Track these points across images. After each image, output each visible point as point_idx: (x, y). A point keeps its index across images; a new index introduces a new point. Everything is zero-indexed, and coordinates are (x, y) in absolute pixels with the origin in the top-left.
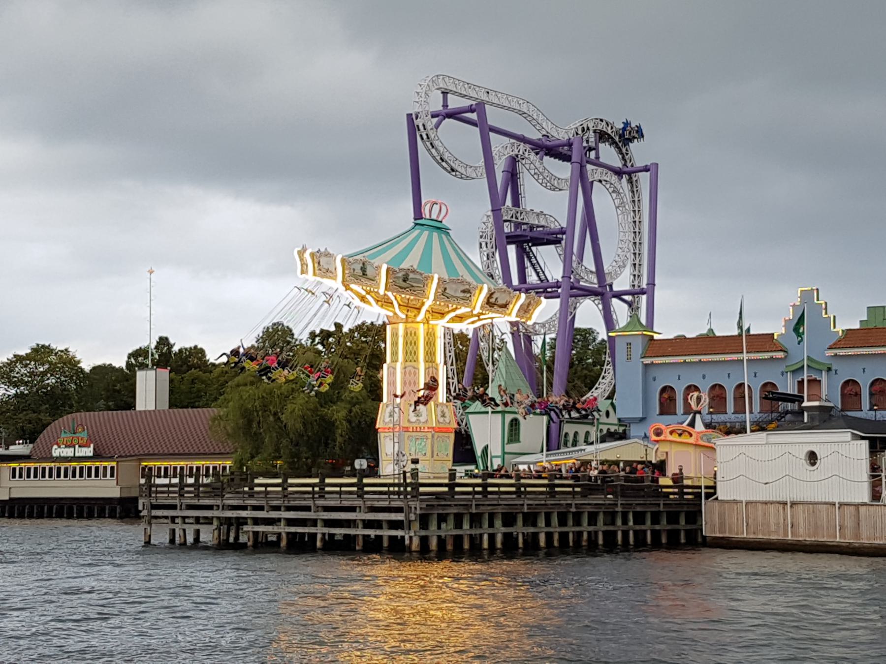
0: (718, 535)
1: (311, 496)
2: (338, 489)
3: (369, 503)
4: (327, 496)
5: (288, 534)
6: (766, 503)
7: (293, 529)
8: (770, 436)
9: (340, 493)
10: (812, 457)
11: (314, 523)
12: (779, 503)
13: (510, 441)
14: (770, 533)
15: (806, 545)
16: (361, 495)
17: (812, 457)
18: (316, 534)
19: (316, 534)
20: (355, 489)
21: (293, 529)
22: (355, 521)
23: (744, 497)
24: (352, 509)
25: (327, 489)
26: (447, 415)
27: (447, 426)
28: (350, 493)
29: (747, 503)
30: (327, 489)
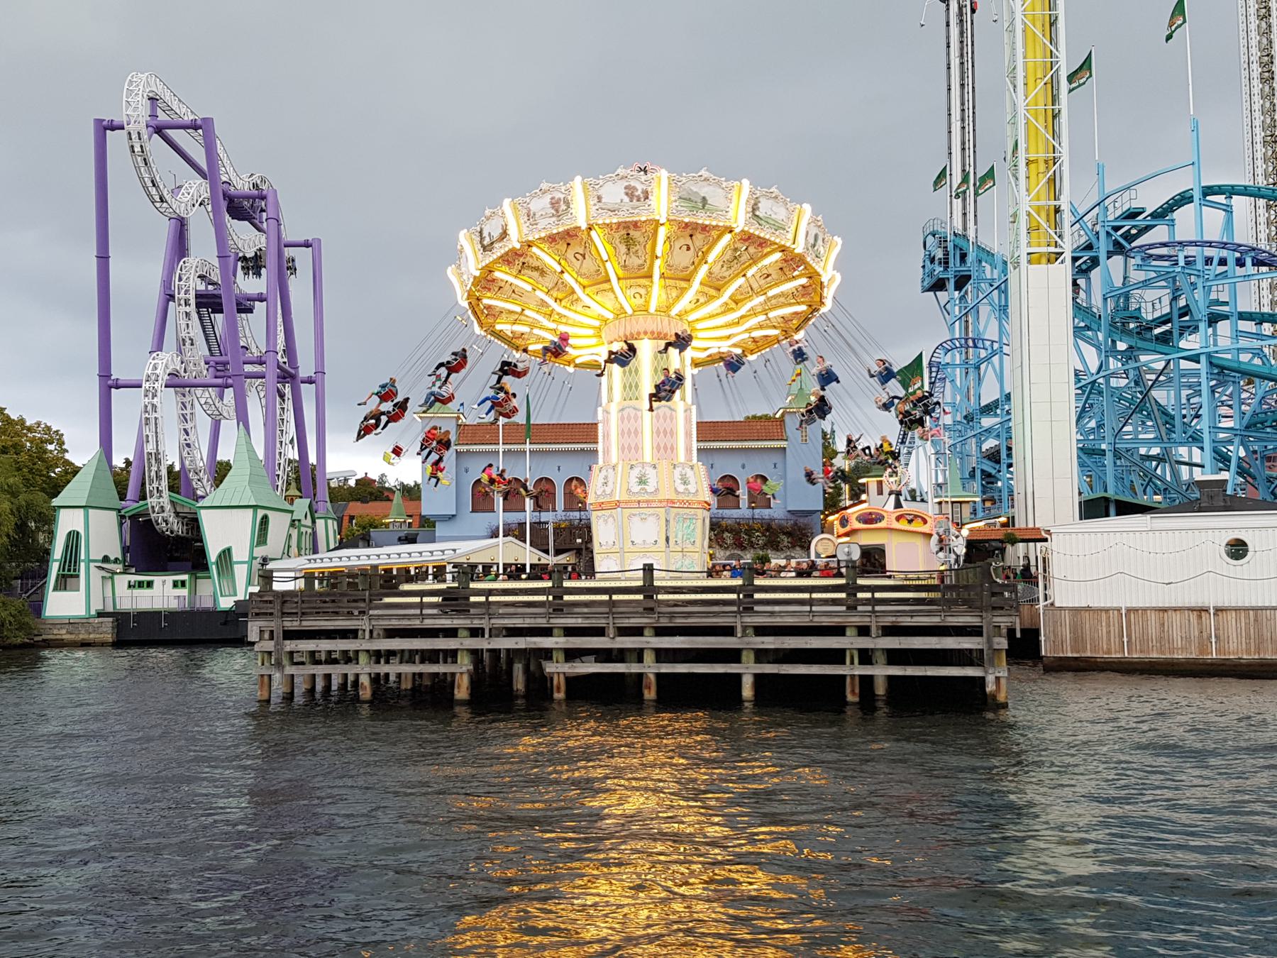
0: (1070, 655)
1: (735, 609)
2: (806, 596)
3: (888, 621)
4: (756, 608)
5: (659, 676)
6: (1165, 610)
7: (666, 668)
8: (1155, 521)
9: (810, 602)
10: (1238, 549)
11: (733, 656)
12: (1192, 609)
13: (259, 544)
14: (1172, 651)
15: (1241, 665)
16: (747, 607)
17: (1238, 549)
18: (738, 678)
19: (738, 678)
20: (843, 595)
21: (666, 668)
22: (841, 652)
23: (1124, 603)
24: (839, 631)
25: (757, 596)
26: (692, 480)
27: (690, 498)
28: (835, 602)
29: (1129, 610)
30: (757, 596)
